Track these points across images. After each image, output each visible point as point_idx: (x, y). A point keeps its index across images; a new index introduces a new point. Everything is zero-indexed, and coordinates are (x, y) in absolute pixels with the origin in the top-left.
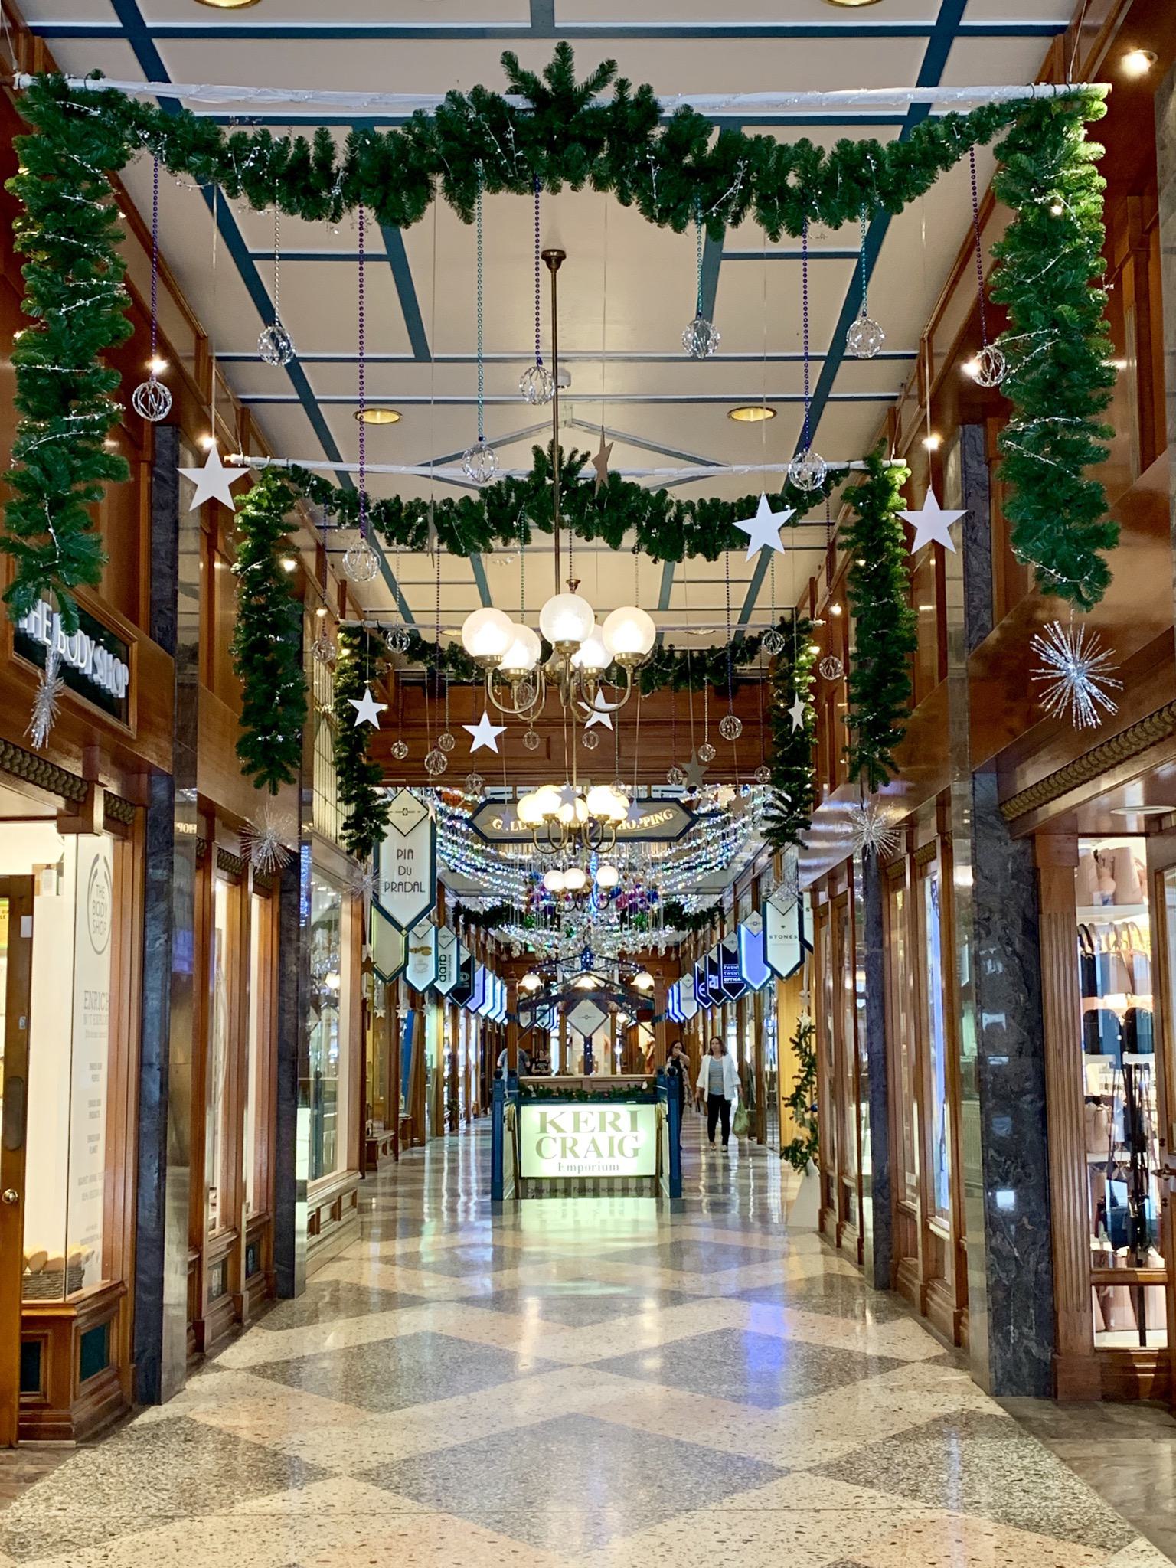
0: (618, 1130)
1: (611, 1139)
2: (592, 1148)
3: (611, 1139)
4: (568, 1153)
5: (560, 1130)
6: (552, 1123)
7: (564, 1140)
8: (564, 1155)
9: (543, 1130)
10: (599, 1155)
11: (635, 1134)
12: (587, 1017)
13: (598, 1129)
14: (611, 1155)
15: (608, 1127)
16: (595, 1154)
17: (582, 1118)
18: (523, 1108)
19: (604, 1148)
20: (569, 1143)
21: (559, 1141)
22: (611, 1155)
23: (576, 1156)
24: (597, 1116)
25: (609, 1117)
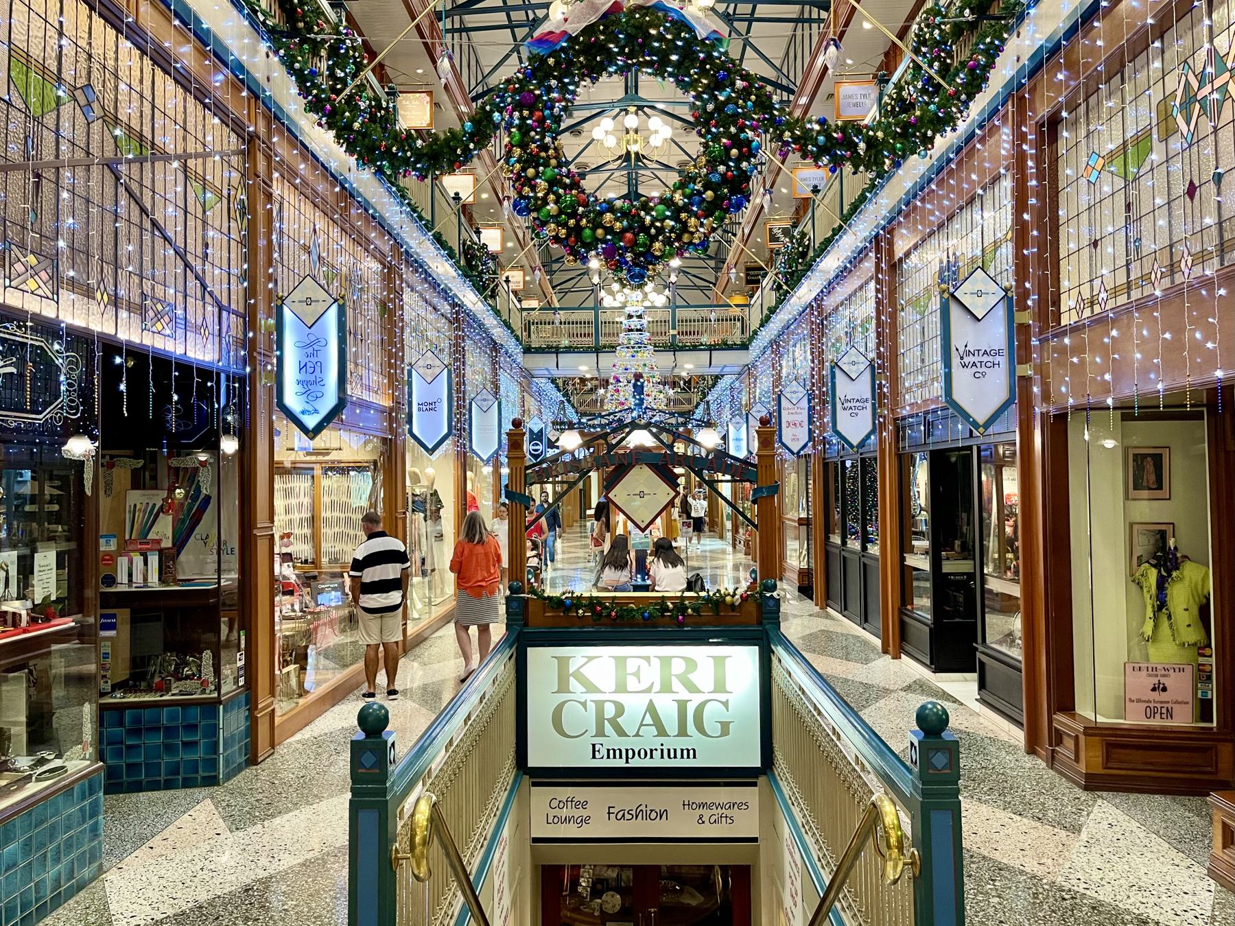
0: (693, 689)
1: (682, 706)
2: (648, 720)
3: (682, 706)
4: (608, 728)
5: (591, 688)
6: (578, 676)
7: (600, 705)
8: (600, 733)
9: (563, 687)
10: (662, 732)
11: (723, 697)
12: (642, 495)
13: (657, 687)
14: (683, 732)
15: (676, 685)
16: (654, 731)
17: (632, 665)
18: (532, 652)
19: (672, 727)
20: (610, 711)
21: (592, 707)
22: (683, 732)
23: (621, 733)
24: (656, 663)
25: (678, 667)
